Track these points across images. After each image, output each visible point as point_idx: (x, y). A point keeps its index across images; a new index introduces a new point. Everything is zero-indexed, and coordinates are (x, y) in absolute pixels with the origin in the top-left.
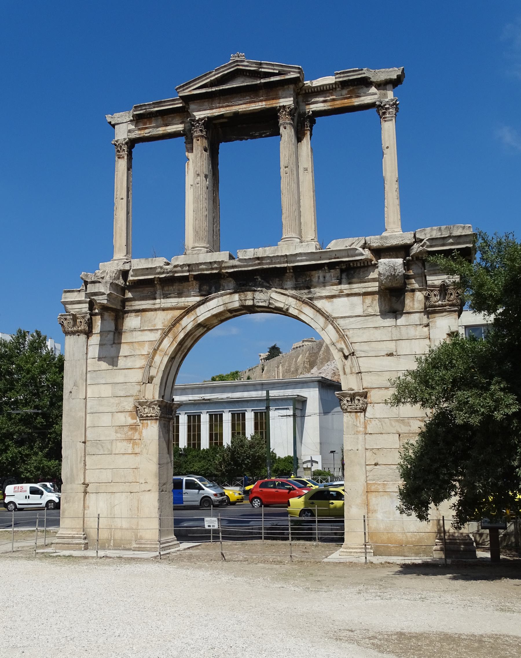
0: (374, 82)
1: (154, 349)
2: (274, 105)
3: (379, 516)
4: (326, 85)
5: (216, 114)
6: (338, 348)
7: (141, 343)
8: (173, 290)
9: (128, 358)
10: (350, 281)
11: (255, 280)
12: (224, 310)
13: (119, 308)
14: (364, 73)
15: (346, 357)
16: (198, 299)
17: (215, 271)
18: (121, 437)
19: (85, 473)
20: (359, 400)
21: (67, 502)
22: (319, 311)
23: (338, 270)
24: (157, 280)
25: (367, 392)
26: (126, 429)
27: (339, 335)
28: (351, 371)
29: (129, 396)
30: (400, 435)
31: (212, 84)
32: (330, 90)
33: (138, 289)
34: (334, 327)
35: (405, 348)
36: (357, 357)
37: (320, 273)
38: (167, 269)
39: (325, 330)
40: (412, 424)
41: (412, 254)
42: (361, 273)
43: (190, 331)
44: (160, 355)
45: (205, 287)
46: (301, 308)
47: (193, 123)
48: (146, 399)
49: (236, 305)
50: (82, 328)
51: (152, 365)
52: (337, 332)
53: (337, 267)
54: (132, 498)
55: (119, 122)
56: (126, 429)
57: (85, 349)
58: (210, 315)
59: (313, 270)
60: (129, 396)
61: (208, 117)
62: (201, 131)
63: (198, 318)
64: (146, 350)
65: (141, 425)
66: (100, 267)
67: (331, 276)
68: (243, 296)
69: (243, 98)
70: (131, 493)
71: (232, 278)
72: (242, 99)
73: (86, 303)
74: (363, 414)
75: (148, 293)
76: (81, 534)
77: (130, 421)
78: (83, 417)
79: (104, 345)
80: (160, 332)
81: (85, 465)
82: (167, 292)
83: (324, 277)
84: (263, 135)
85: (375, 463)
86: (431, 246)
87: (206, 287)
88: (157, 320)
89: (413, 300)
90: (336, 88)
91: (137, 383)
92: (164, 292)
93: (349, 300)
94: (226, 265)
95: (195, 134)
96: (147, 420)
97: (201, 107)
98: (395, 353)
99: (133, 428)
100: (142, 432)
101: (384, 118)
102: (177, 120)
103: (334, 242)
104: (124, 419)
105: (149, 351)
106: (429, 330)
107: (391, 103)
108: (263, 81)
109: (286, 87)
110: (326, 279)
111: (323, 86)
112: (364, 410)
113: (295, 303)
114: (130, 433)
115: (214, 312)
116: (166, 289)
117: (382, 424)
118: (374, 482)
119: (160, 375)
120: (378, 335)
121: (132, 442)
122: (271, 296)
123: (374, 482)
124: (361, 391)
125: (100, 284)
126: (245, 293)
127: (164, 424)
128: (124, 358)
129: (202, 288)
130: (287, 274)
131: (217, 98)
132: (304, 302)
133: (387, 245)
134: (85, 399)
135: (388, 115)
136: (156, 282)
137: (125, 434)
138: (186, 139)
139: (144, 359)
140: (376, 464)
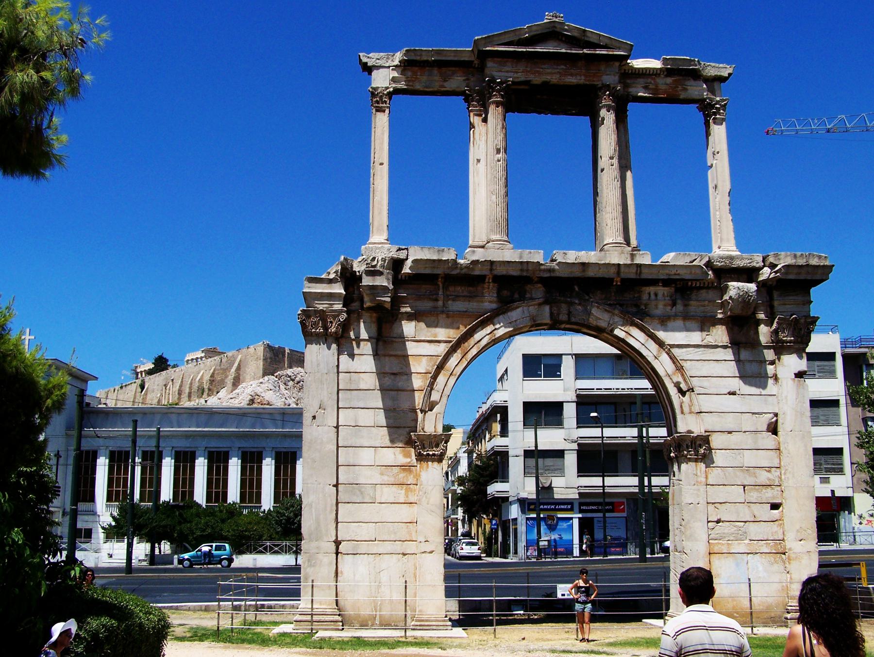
4: (650, 69)
5: (523, 79)
6: (675, 381)
9: (398, 376)
13: (389, 309)
16: (494, 306)
17: (525, 274)
18: (388, 481)
19: (337, 527)
21: (310, 566)
23: (673, 288)
24: (442, 278)
26: (396, 469)
28: (690, 409)
30: (744, 487)
32: (653, 74)
33: (411, 286)
37: (652, 289)
38: (461, 265)
39: (659, 359)
40: (757, 475)
43: (486, 346)
44: (445, 375)
48: (425, 432)
52: (674, 363)
53: (673, 285)
54: (406, 561)
66: (363, 252)
70: (404, 554)
72: (555, 67)
76: (335, 609)
78: (334, 451)
83: (656, 295)
85: (718, 520)
87: (505, 293)
90: (659, 74)
92: (448, 293)
98: (738, 392)
99: (406, 468)
100: (420, 475)
103: (672, 254)
104: (393, 456)
105: (428, 368)
106: (776, 367)
108: (585, 51)
111: (646, 69)
114: (402, 475)
116: (451, 289)
117: (725, 474)
121: (404, 488)
123: (716, 541)
128: (392, 377)
134: (337, 427)
135: (718, 116)
136: (440, 280)
139: (420, 378)
140: (718, 521)
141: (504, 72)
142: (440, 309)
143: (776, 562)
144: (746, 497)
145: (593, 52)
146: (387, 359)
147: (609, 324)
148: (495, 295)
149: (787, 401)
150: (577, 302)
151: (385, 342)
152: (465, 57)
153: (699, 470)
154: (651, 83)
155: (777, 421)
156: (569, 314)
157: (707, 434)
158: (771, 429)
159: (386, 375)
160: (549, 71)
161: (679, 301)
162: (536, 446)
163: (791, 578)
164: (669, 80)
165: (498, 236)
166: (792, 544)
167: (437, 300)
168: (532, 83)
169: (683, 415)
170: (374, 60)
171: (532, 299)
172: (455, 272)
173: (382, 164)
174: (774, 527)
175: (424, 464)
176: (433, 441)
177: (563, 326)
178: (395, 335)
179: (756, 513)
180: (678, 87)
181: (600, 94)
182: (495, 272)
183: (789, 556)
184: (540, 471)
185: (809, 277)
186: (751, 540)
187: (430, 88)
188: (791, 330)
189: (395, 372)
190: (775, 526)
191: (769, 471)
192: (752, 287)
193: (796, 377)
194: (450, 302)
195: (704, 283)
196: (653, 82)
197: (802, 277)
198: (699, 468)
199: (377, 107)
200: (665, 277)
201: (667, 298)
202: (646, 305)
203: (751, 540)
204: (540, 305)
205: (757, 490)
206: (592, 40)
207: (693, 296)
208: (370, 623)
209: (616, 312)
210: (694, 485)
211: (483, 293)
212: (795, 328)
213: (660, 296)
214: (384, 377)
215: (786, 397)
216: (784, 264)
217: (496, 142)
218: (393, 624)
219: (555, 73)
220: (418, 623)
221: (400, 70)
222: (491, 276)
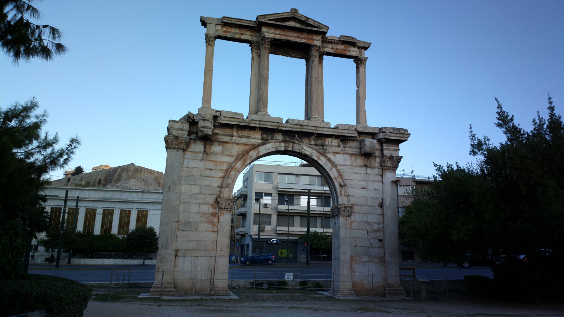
0: (357, 46)
1: (232, 167)
2: (311, 43)
3: (357, 274)
7: (222, 163)
8: (244, 133)
9: (212, 171)
12: (276, 151)
14: (355, 40)
16: (260, 141)
20: (348, 210)
21: (161, 262)
22: (329, 160)
26: (208, 215)
27: (339, 174)
28: (345, 194)
29: (211, 195)
31: (277, 20)
32: (336, 43)
34: (336, 170)
35: (371, 185)
42: (351, 143)
44: (234, 171)
45: (265, 135)
46: (319, 157)
47: (264, 39)
48: (224, 197)
49: (283, 149)
50: (182, 147)
51: (230, 176)
52: (338, 172)
55: (210, 23)
56: (208, 215)
57: (182, 160)
58: (267, 152)
60: (211, 195)
61: (274, 39)
63: (259, 153)
64: (224, 167)
65: (219, 214)
67: (335, 142)
71: (281, 133)
72: (293, 34)
73: (186, 131)
74: (349, 218)
75: (228, 132)
77: (212, 210)
79: (196, 159)
80: (235, 157)
81: (177, 238)
83: (332, 142)
84: (297, 57)
87: (265, 136)
88: (233, 149)
89: (375, 162)
90: (339, 43)
91: (217, 187)
92: (238, 133)
93: (344, 157)
94: (282, 125)
95: (265, 46)
96: (224, 210)
98: (366, 188)
99: (213, 215)
100: (220, 218)
101: (361, 66)
104: (207, 208)
107: (365, 59)
108: (308, 28)
109: (318, 35)
110: (333, 143)
112: (350, 216)
113: (316, 153)
114: (211, 218)
115: (270, 151)
116: (240, 132)
117: (359, 225)
118: (354, 255)
120: (357, 177)
121: (212, 224)
122: (303, 147)
124: (350, 206)
125: (208, 122)
126: (289, 143)
128: (210, 170)
129: (263, 136)
130: (313, 137)
131: (279, 29)
132: (321, 154)
133: (366, 131)
135: (362, 65)
136: (235, 127)
137: (208, 218)
141: (270, 33)
147: (310, 153)
148: (260, 137)
149: (387, 193)
150: (297, 142)
151: (207, 153)
153: (347, 222)
154: (334, 47)
156: (293, 147)
157: (352, 206)
162: (260, 212)
164: (343, 47)
166: (388, 258)
167: (233, 136)
168: (282, 40)
169: (341, 196)
172: (242, 124)
177: (289, 153)
178: (212, 152)
179: (372, 243)
180: (346, 50)
184: (261, 223)
185: (400, 139)
189: (211, 168)
196: (335, 46)
198: (347, 221)
199: (208, 43)
204: (280, 142)
208: (189, 292)
212: (392, 161)
213: (333, 143)
214: (206, 171)
215: (387, 191)
218: (201, 292)
219: (293, 37)
220: (214, 292)
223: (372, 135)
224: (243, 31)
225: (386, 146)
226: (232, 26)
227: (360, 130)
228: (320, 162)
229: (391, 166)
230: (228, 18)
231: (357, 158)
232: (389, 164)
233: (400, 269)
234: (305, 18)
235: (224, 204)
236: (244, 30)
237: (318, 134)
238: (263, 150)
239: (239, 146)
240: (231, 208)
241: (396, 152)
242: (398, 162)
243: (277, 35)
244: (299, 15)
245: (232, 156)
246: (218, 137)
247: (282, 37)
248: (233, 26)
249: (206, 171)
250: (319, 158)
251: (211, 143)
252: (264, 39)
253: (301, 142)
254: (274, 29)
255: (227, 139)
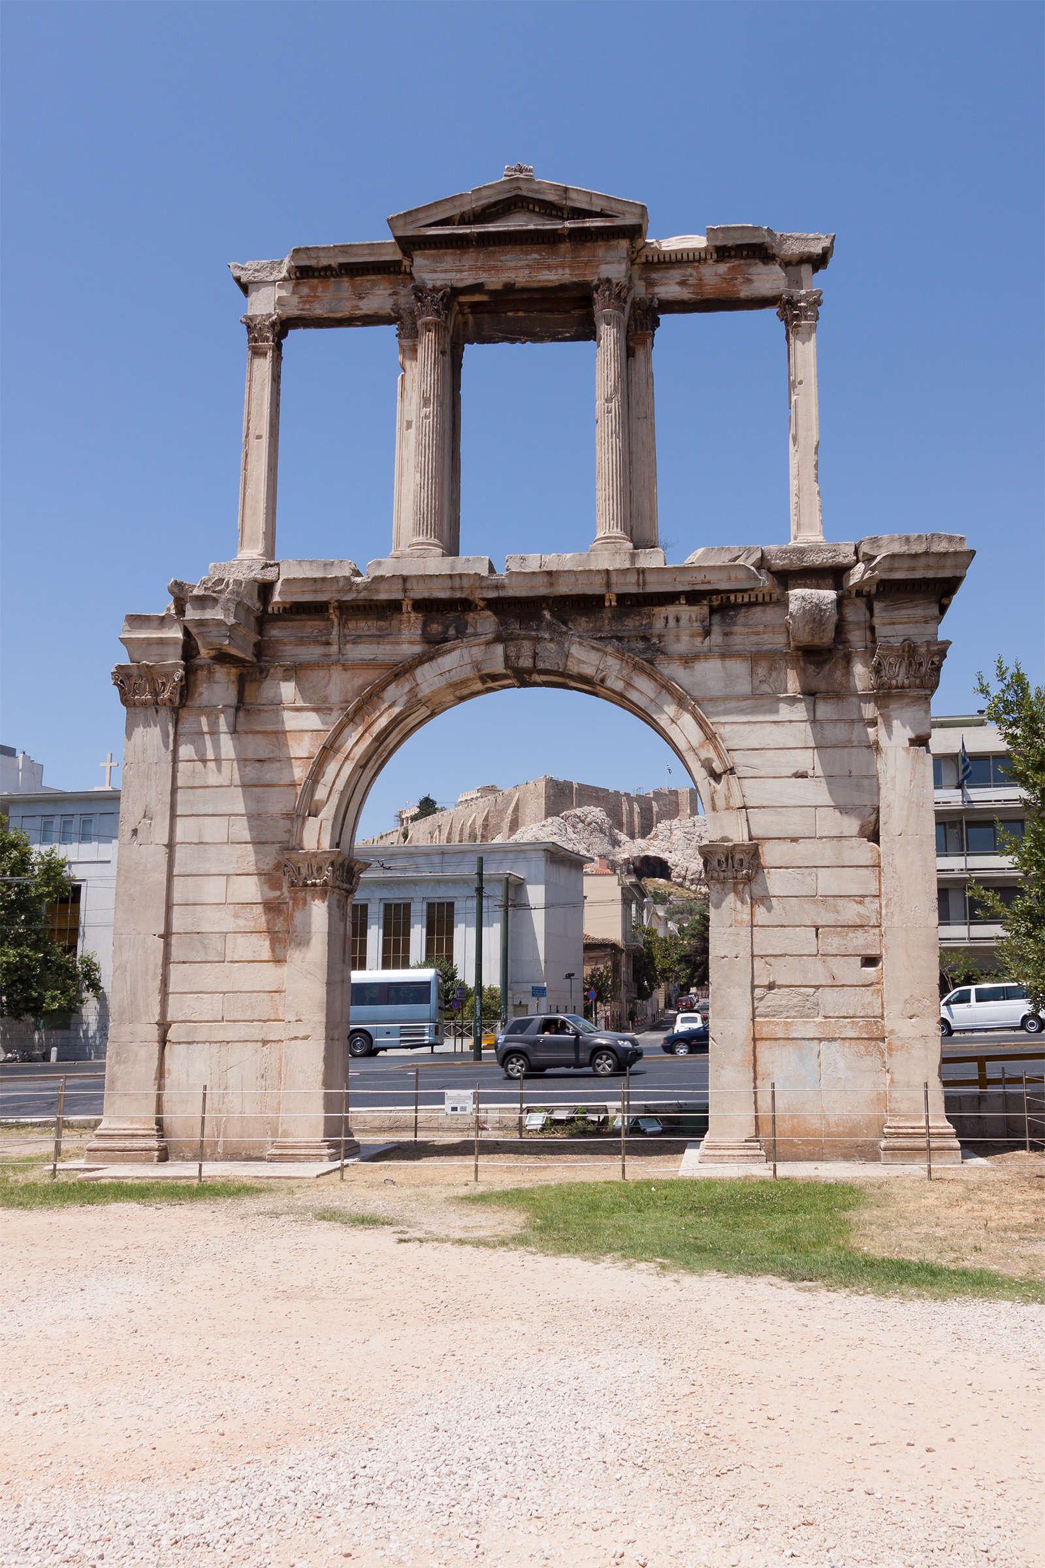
5: (470, 281)
6: (702, 758)
9: (265, 764)
10: (727, 629)
11: (540, 618)
15: (716, 777)
16: (417, 649)
17: (458, 595)
20: (741, 860)
24: (334, 608)
25: (757, 845)
28: (728, 803)
31: (464, 220)
33: (290, 624)
36: (739, 778)
37: (671, 610)
38: (358, 585)
39: (678, 722)
41: (851, 583)
46: (631, 678)
53: (705, 602)
59: (655, 605)
61: (453, 289)
62: (437, 311)
63: (417, 689)
68: (513, 649)
69: (527, 255)
74: (747, 887)
82: (353, 632)
83: (678, 620)
85: (770, 983)
86: (891, 570)
87: (435, 628)
92: (346, 631)
93: (724, 667)
94: (484, 584)
97: (438, 265)
98: (811, 773)
102: (382, 287)
110: (682, 623)
116: (352, 625)
119: (335, 799)
123: (767, 1019)
124: (747, 842)
127: (339, 901)
128: (258, 765)
129: (428, 629)
131: (471, 250)
132: (637, 667)
136: (331, 611)
138: (401, 329)
140: (771, 986)
141: (441, 272)
142: (334, 658)
143: (868, 1053)
144: (820, 944)
145: (580, 225)
146: (250, 736)
147: (598, 669)
148: (420, 632)
149: (894, 785)
150: (547, 636)
152: (386, 254)
155: (878, 817)
156: (535, 656)
158: (867, 833)
159: (248, 763)
160: (511, 264)
161: (716, 629)
163: (892, 1080)
165: (421, 538)
166: (897, 1024)
167: (328, 644)
170: (251, 272)
171: (475, 635)
172: (348, 597)
173: (259, 437)
174: (868, 995)
175: (301, 895)
176: (313, 862)
181: (595, 295)
182: (412, 595)
183: (889, 1044)
185: (930, 574)
186: (826, 1017)
187: (335, 312)
188: (904, 665)
189: (262, 757)
190: (869, 993)
191: (860, 903)
192: (830, 595)
193: (911, 745)
194: (349, 646)
195: (757, 595)
197: (918, 575)
200: (687, 588)
201: (696, 624)
202: (660, 637)
203: (826, 1017)
204: (488, 643)
205: (839, 934)
206: (578, 205)
207: (741, 619)
209: (610, 649)
210: (731, 926)
211: (400, 630)
212: (910, 664)
213: (684, 622)
214: (245, 767)
216: (884, 555)
217: (424, 387)
219: (521, 268)
221: (290, 286)
222: (410, 603)
223: (834, 575)
224: (364, 281)
225: (885, 609)
226: (326, 277)
227: (778, 563)
228: (634, 696)
229: (906, 682)
230: (308, 249)
231: (775, 668)
232: (899, 675)
233: (945, 1061)
234: (559, 193)
235: (304, 871)
236: (368, 281)
237: (621, 598)
238: (429, 678)
239: (348, 674)
240: (325, 883)
241: (929, 628)
242: (933, 663)
243: (466, 273)
244: (536, 187)
245: (331, 709)
246: (282, 651)
247: (483, 278)
248: (328, 273)
249: (247, 769)
250: (629, 685)
251: (261, 673)
252: (419, 292)
253: (566, 633)
254: (455, 254)
255: (313, 652)
